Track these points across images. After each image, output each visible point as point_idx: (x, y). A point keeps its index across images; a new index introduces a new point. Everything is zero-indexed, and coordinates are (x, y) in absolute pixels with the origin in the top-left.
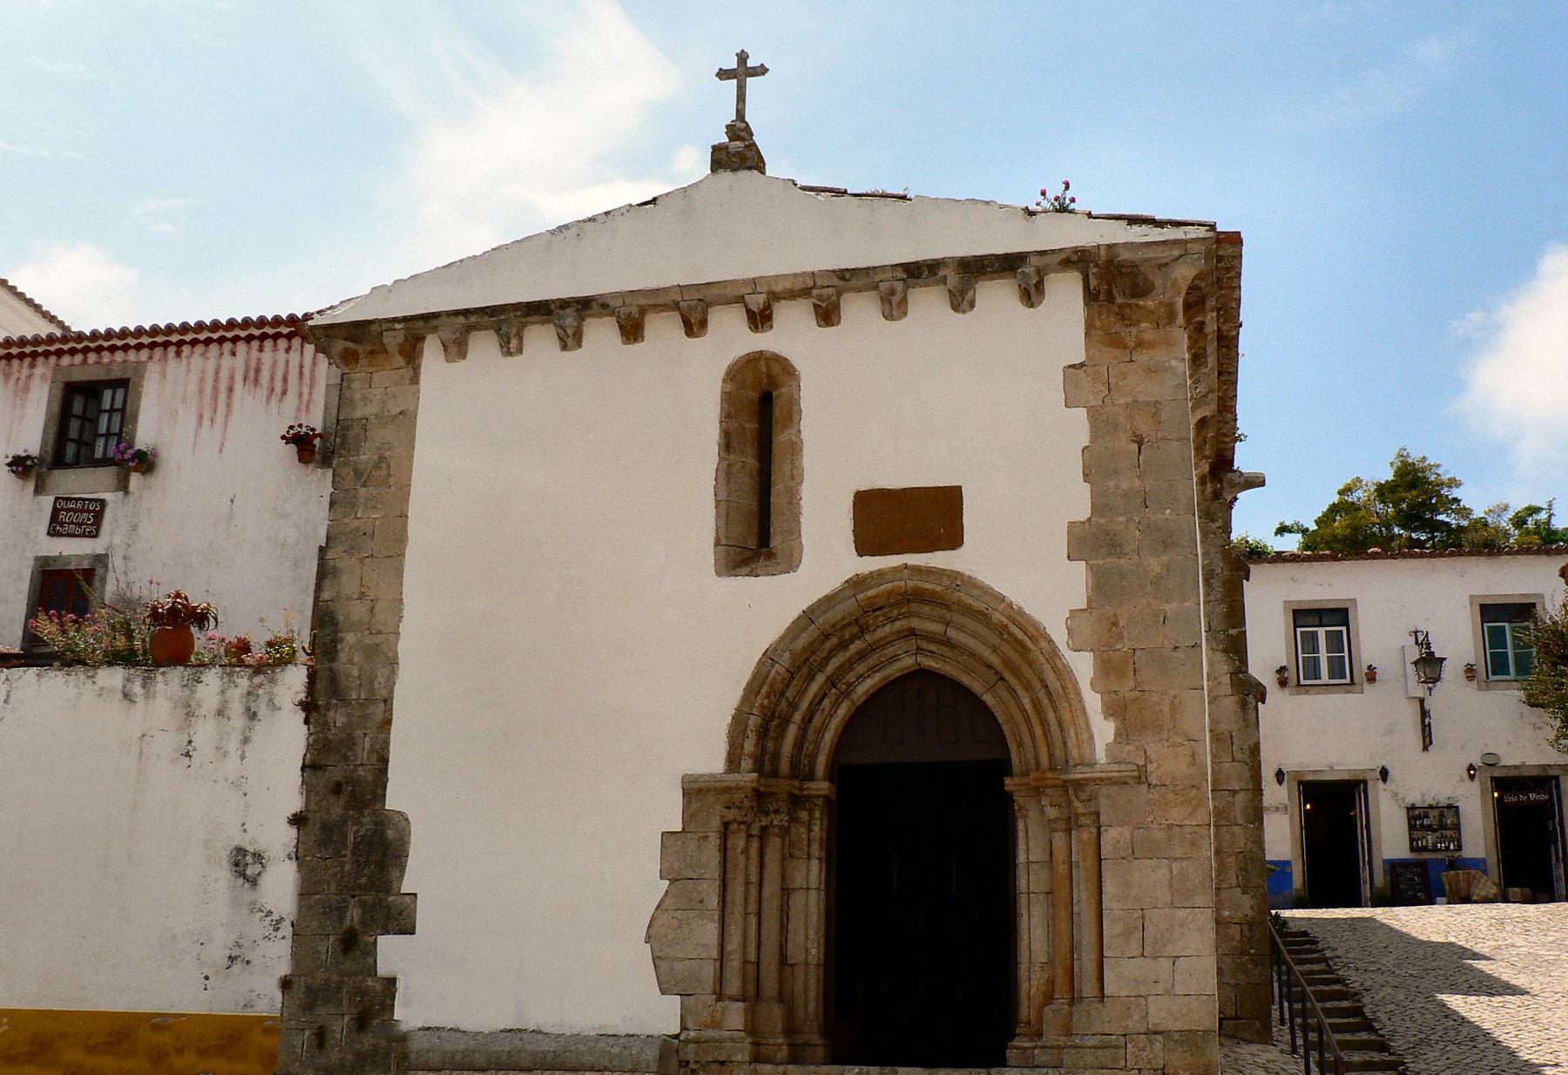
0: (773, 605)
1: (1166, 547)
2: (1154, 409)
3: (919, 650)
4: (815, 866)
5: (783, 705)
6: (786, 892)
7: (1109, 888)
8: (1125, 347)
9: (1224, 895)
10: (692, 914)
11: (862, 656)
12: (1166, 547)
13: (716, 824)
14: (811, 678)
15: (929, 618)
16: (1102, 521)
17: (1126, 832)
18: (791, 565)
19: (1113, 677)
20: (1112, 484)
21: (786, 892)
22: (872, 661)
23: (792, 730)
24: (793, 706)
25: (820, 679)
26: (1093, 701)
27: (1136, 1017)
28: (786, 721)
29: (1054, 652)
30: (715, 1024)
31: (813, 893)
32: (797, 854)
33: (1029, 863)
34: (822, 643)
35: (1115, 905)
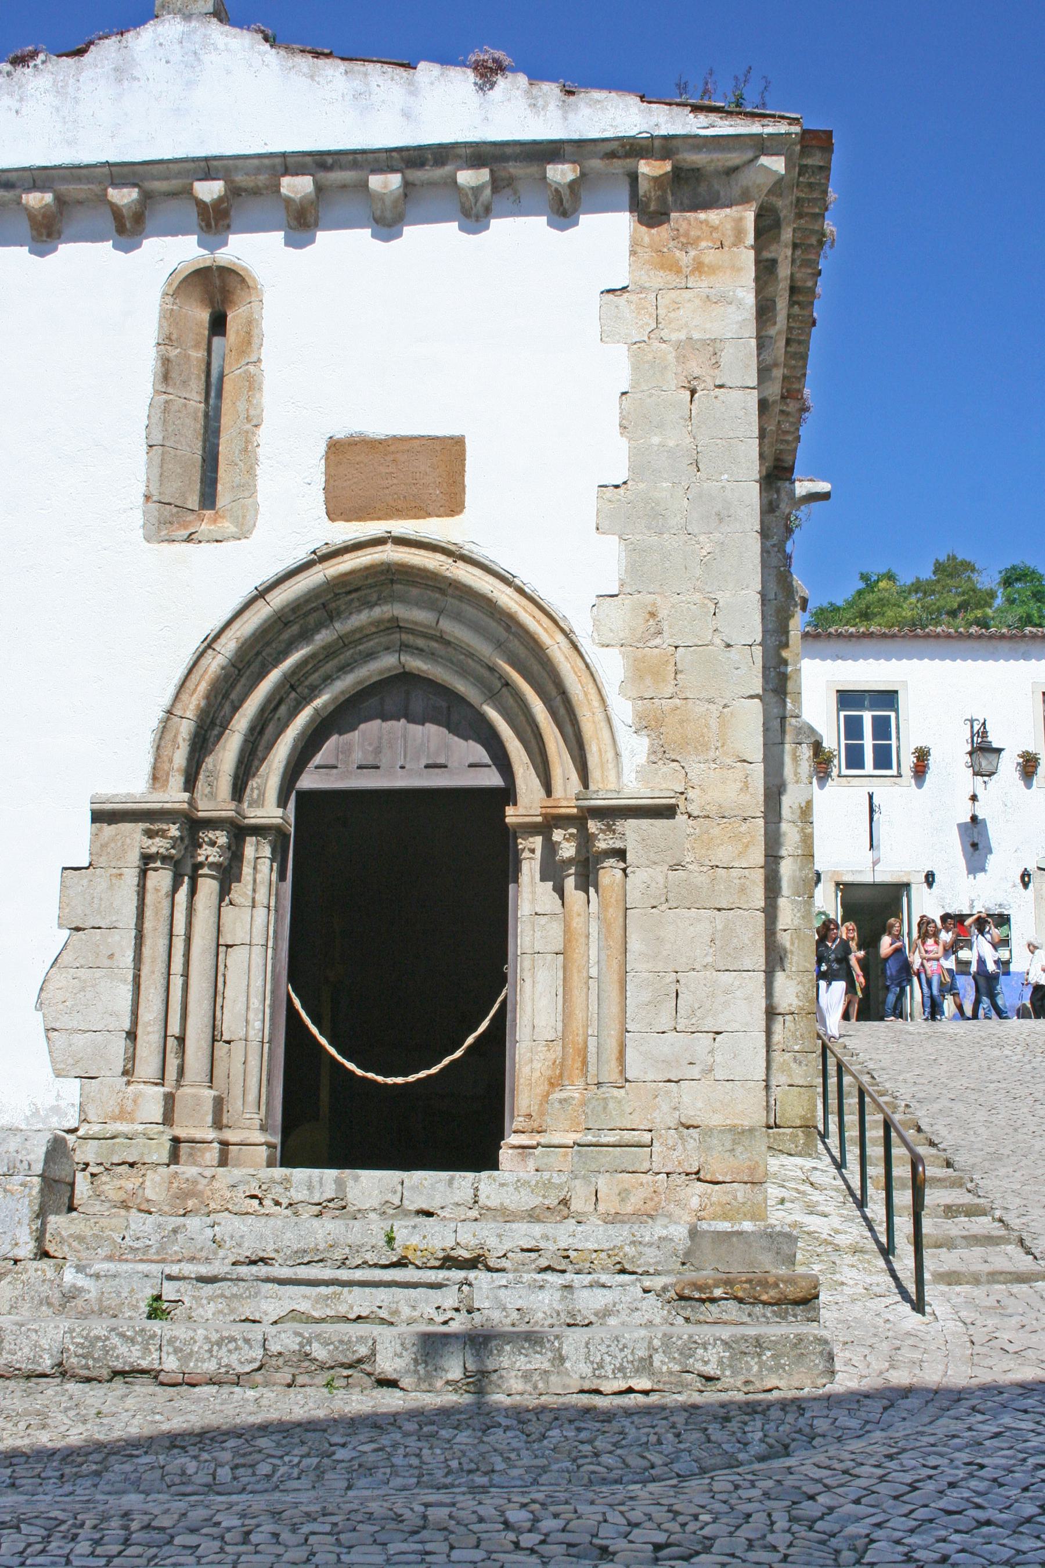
0: (221, 581)
1: (721, 520)
2: (712, 348)
4: (261, 913)
7: (635, 944)
8: (679, 272)
10: (98, 973)
11: (329, 652)
12: (721, 520)
13: (134, 858)
15: (418, 604)
16: (642, 486)
19: (648, 681)
20: (656, 440)
22: (343, 658)
25: (274, 676)
26: (622, 710)
27: (665, 1108)
30: (123, 1115)
31: (258, 951)
34: (280, 632)
35: (639, 967)
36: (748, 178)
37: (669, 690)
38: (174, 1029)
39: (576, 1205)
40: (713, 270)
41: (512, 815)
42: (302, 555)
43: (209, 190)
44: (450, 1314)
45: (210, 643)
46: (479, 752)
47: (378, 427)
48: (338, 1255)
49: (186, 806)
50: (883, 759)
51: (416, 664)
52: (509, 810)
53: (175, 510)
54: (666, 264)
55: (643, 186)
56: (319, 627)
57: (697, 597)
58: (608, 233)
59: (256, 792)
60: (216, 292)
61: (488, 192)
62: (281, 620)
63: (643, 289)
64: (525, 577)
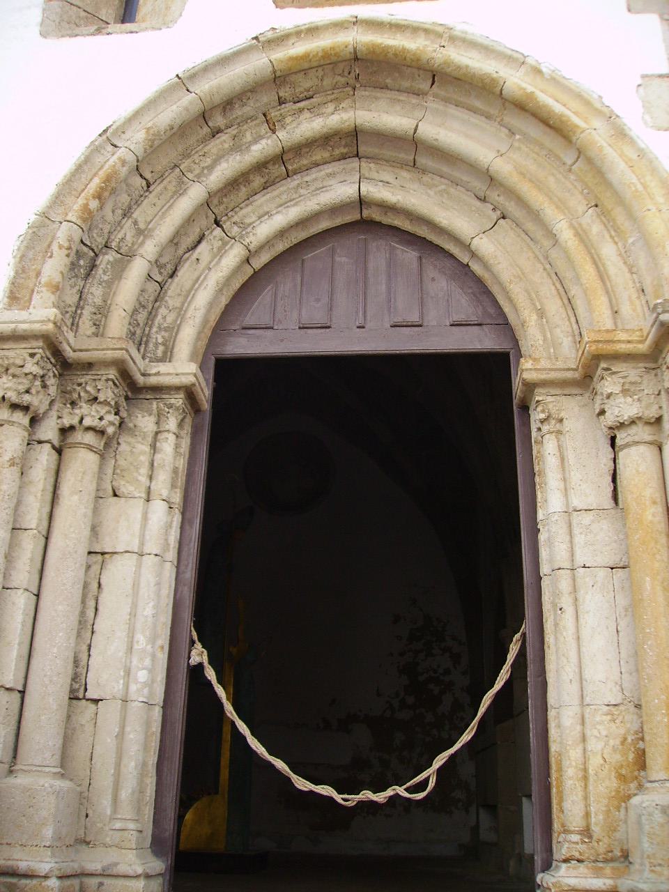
4: (158, 510)
5: (127, 230)
6: (98, 556)
14: (180, 191)
18: (165, 19)
21: (98, 556)
23: (137, 269)
24: (142, 233)
25: (195, 194)
28: (129, 256)
29: (621, 134)
31: (149, 561)
32: (125, 488)
33: (569, 512)
41: (527, 370)
46: (464, 307)
49: (50, 326)
53: (84, 14)
56: (256, 141)
59: (161, 348)
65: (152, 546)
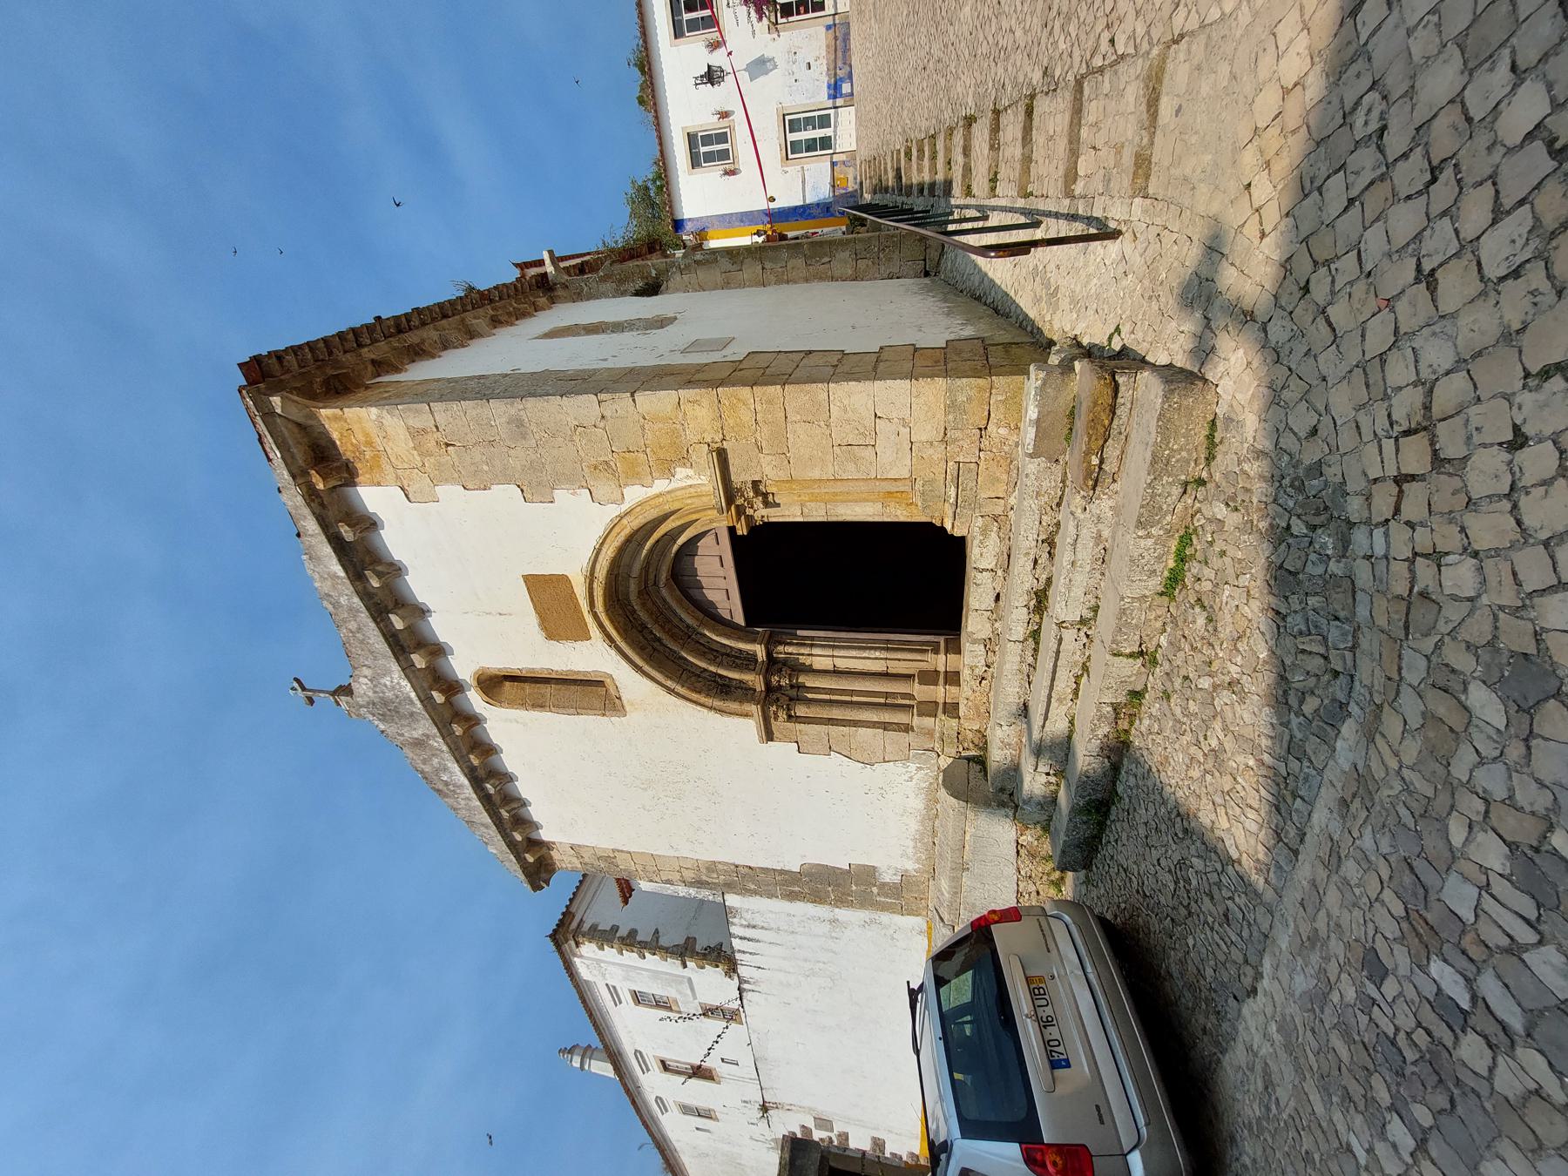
2: (416, 434)
3: (655, 584)
4: (816, 651)
9: (837, 274)
17: (765, 460)
26: (661, 485)
27: (931, 451)
36: (296, 414)
37: (642, 455)
38: (882, 700)
39: (999, 510)
40: (367, 435)
42: (613, 652)
43: (439, 698)
44: (1082, 634)
45: (671, 691)
47: (533, 619)
48: (1025, 668)
50: (722, 138)
51: (664, 576)
52: (739, 533)
54: (375, 465)
55: (332, 483)
57: (576, 438)
58: (372, 497)
60: (492, 684)
61: (379, 568)
62: (649, 659)
63: (398, 477)
64: (593, 543)
65: (829, 652)
